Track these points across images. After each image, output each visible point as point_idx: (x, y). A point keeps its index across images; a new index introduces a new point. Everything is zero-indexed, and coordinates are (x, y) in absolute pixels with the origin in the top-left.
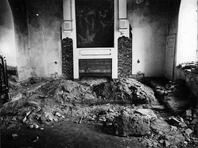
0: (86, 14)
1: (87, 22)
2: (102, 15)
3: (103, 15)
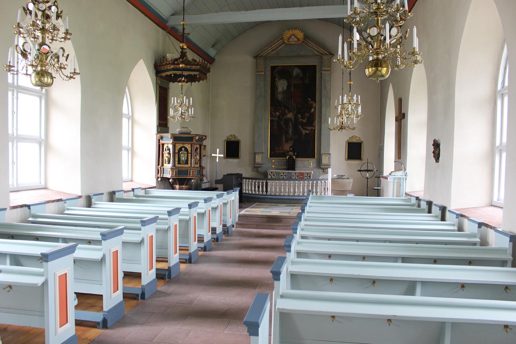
3: (302, 119)
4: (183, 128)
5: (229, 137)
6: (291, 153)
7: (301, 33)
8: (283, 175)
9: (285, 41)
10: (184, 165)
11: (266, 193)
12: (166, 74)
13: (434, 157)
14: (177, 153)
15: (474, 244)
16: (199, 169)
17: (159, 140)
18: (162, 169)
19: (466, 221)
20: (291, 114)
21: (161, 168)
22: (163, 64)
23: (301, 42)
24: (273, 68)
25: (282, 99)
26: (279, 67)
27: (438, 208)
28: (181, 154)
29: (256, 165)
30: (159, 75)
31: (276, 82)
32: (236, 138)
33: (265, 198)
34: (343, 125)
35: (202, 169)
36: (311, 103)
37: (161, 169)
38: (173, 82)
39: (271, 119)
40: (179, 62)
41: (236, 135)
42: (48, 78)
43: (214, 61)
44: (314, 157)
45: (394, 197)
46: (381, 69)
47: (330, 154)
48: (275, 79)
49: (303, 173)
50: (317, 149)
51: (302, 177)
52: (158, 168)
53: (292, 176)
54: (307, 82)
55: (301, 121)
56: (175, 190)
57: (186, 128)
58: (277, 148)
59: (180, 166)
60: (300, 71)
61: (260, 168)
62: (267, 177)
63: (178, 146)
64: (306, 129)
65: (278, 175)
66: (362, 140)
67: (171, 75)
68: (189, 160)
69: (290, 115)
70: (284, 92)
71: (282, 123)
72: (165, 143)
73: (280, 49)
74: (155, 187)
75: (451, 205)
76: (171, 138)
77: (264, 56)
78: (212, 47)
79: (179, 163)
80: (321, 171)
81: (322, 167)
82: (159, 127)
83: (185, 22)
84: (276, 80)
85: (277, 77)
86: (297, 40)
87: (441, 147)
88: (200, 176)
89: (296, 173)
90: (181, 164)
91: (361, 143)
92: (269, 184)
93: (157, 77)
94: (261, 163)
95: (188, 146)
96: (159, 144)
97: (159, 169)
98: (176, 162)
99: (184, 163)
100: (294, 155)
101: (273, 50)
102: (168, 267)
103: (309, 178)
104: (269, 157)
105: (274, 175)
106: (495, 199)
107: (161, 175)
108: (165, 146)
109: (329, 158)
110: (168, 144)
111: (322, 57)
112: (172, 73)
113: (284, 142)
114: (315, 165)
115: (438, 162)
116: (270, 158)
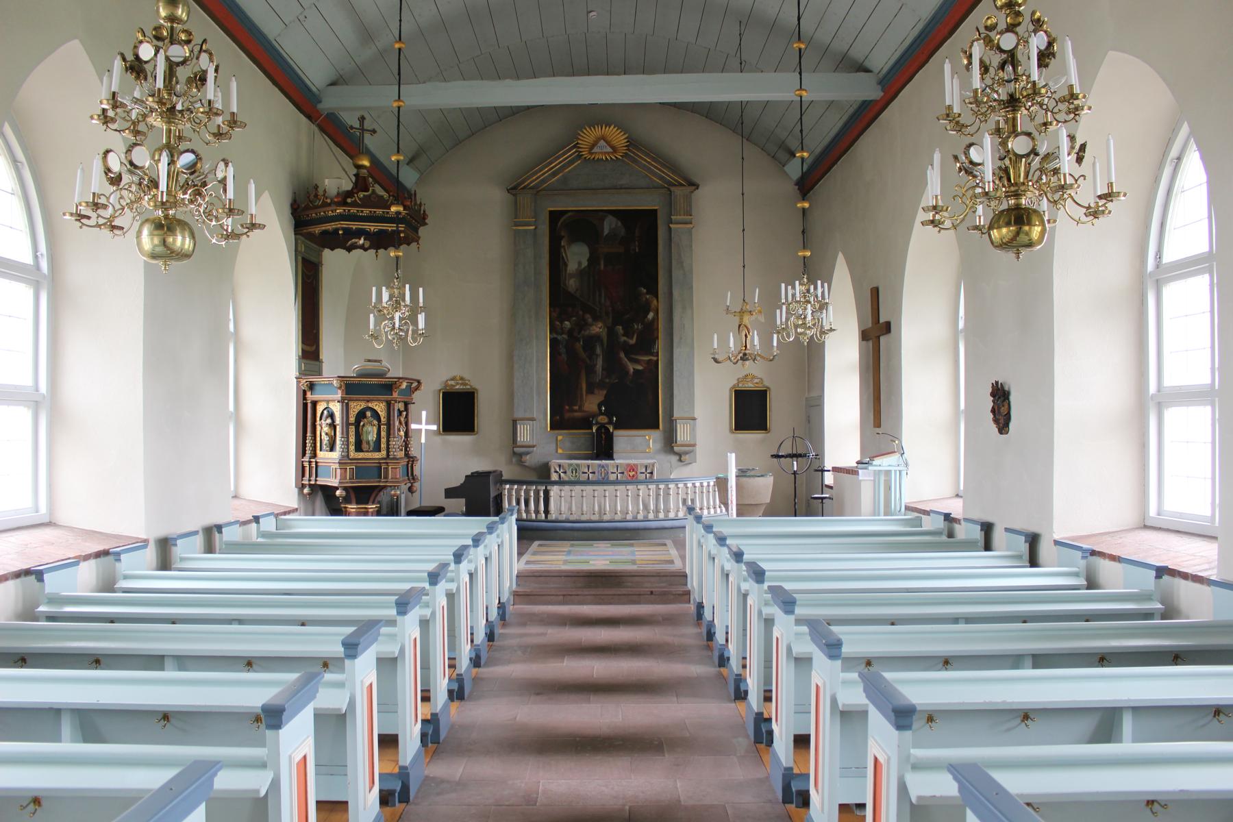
0: (579, 332)
1: (583, 355)
2: (625, 338)
3: (628, 337)
4: (369, 361)
5: (450, 383)
6: (603, 419)
7: (622, 133)
8: (586, 470)
9: (583, 153)
10: (370, 454)
11: (546, 517)
12: (324, 228)
13: (996, 421)
14: (352, 424)
15: (1148, 615)
16: (406, 463)
17: (305, 392)
18: (313, 465)
19: (1104, 565)
20: (600, 324)
21: (310, 462)
22: (316, 204)
23: (621, 156)
24: (554, 216)
25: (577, 290)
26: (570, 214)
27: (1023, 538)
28: (364, 425)
29: (516, 450)
30: (305, 231)
31: (562, 250)
32: (466, 384)
33: (556, 529)
34: (747, 352)
35: (413, 461)
36: (646, 299)
37: (310, 465)
38: (332, 250)
39: (552, 337)
40: (355, 200)
41: (466, 376)
42: (184, 238)
44: (657, 427)
45: (879, 515)
46: (1030, 229)
47: (694, 419)
48: (561, 243)
49: (636, 465)
50: (664, 409)
51: (633, 476)
52: (303, 462)
53: (610, 473)
54: (637, 250)
55: (625, 341)
56: (346, 515)
57: (375, 361)
58: (567, 407)
59: (361, 455)
60: (619, 224)
61: (528, 457)
62: (549, 476)
63: (356, 407)
64: (637, 362)
65: (576, 472)
66: (766, 383)
67: (337, 230)
68: (382, 440)
69: (597, 329)
70: (581, 273)
71: (579, 346)
72: (321, 399)
73: (569, 172)
74: (297, 509)
75: (1055, 530)
76: (340, 388)
77: (530, 188)
78: (408, 164)
79: (359, 448)
80: (674, 459)
81: (676, 449)
83: (402, 101)
84: (562, 244)
85: (563, 237)
86: (611, 150)
87: (1012, 398)
89: (617, 467)
90: (363, 451)
91: (766, 391)
92: (552, 493)
93: (298, 236)
94: (531, 444)
95: (380, 408)
96: (304, 403)
97: (306, 464)
98: (350, 447)
99: (371, 449)
100: (610, 422)
101: (554, 174)
102: (432, 714)
103: (651, 477)
104: (549, 429)
105: (565, 473)
106: (1152, 512)
107: (310, 480)
108: (320, 408)
109: (693, 430)
110: (328, 402)
111: (670, 191)
112: (339, 226)
113: (584, 393)
114: (659, 445)
115: (1007, 433)
116: (552, 432)
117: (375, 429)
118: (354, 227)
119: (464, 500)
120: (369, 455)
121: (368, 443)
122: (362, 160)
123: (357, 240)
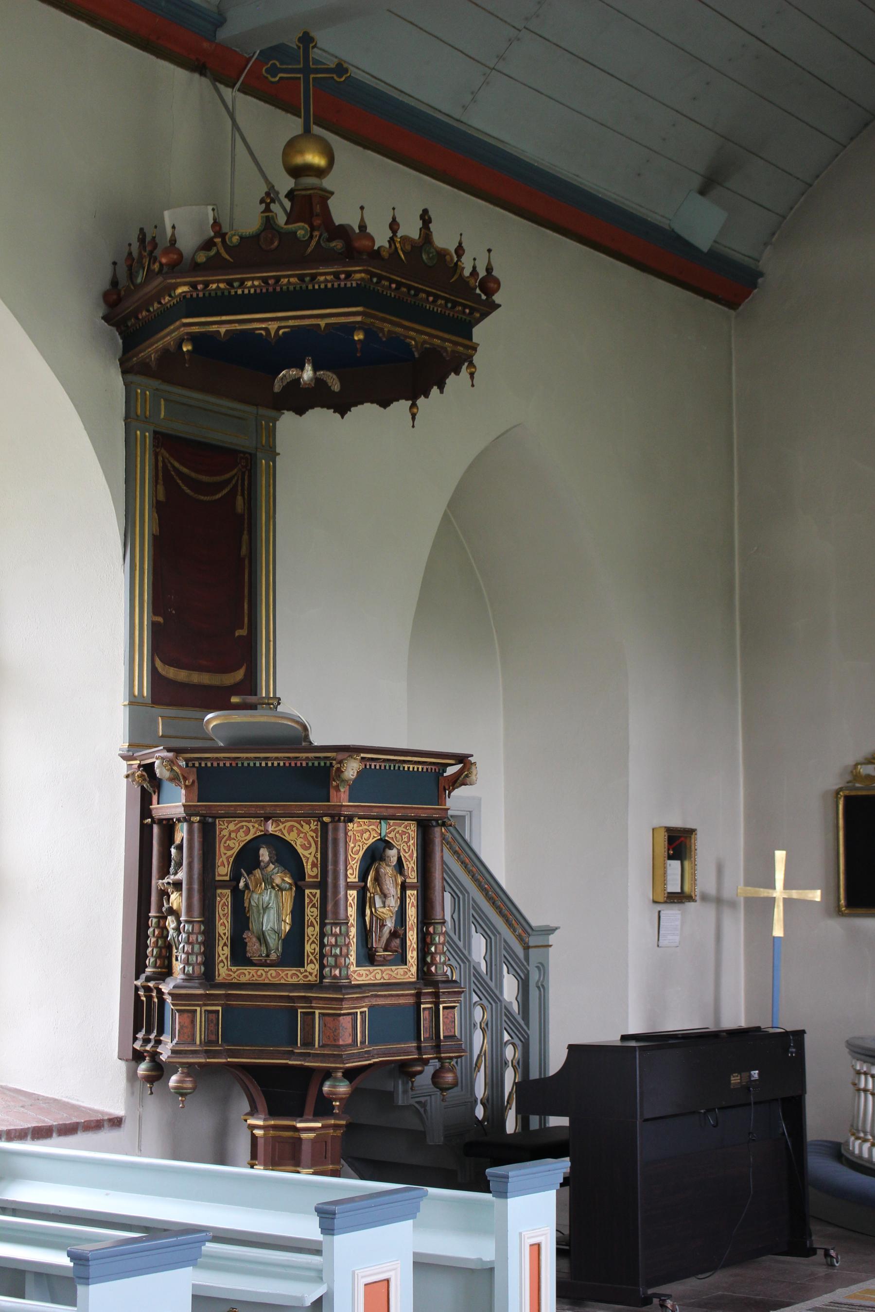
5: (864, 770)
10: (272, 971)
14: (223, 885)
16: (411, 1000)
38: (300, 412)
40: (218, 253)
43: (755, 286)
59: (247, 974)
68: (309, 931)
74: (116, 1122)
78: (703, 192)
79: (239, 956)
82: (158, 710)
88: (419, 1048)
90: (249, 963)
93: (131, 377)
99: (273, 956)
117: (288, 899)
118: (223, 329)
119: (568, 1118)
120: (270, 975)
121: (262, 938)
122: (302, 152)
123: (293, 372)
